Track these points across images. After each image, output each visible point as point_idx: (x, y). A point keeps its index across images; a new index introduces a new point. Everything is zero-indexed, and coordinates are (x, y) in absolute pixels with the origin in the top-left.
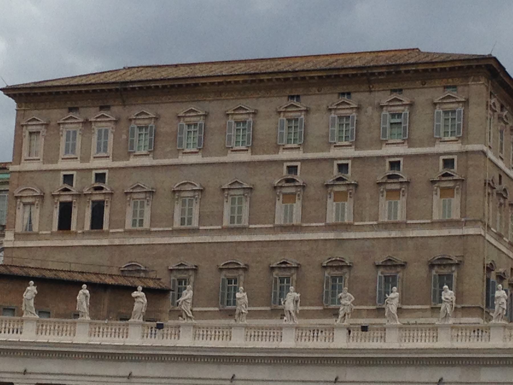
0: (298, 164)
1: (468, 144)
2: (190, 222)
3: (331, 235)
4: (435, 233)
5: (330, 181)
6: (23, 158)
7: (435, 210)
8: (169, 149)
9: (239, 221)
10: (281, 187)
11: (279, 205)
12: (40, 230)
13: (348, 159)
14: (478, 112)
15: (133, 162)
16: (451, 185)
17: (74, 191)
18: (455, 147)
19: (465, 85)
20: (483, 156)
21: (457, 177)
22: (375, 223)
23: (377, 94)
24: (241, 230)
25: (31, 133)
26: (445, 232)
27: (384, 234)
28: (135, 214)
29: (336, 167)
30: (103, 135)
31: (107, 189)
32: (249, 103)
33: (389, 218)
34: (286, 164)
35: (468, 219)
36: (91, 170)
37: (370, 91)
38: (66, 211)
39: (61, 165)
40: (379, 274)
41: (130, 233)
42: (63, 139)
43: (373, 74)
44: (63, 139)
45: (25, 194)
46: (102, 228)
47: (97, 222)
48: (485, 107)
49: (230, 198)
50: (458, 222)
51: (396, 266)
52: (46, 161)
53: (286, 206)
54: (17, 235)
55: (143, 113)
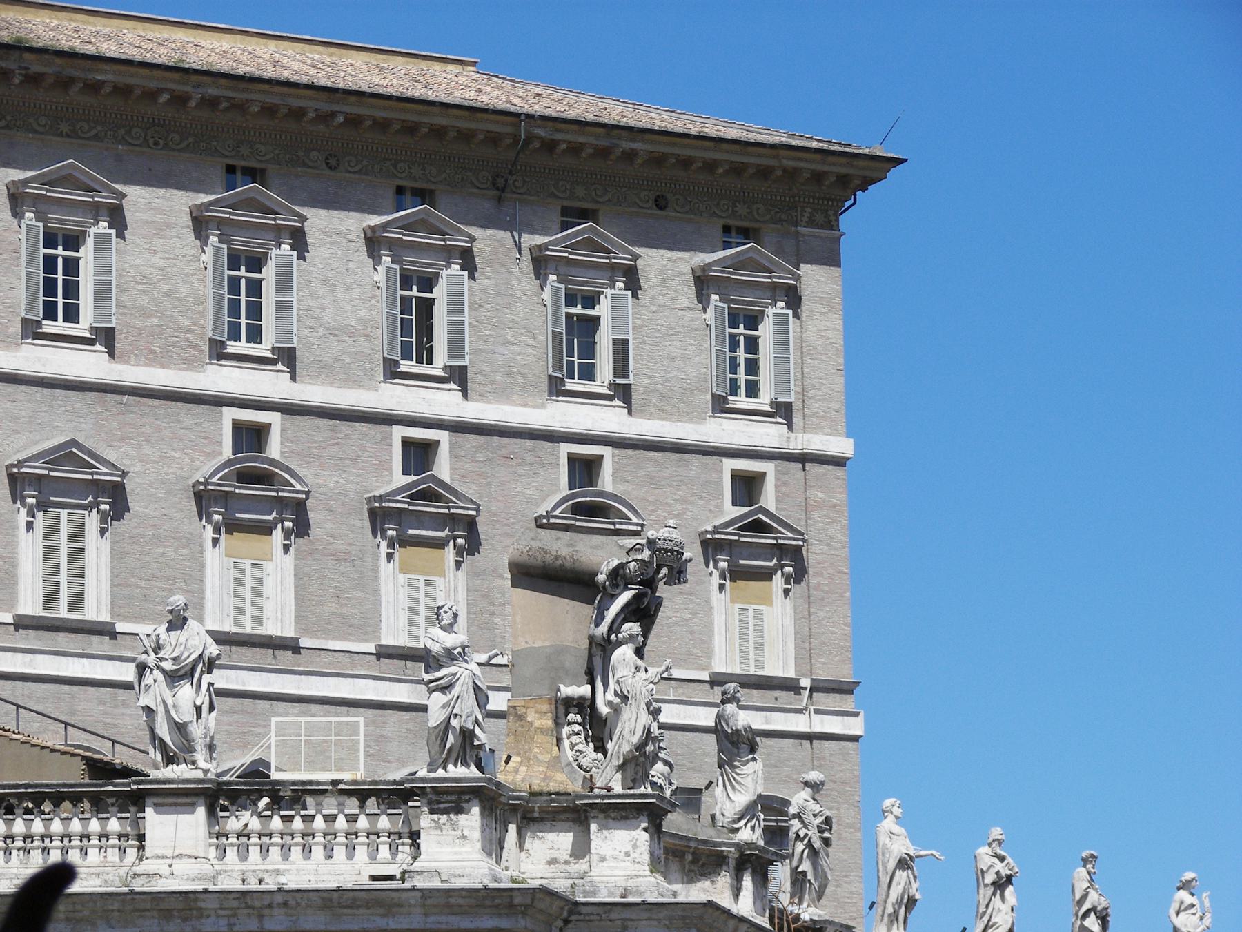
1: (805, 429)
7: (718, 643)
18: (769, 435)
50: (790, 686)
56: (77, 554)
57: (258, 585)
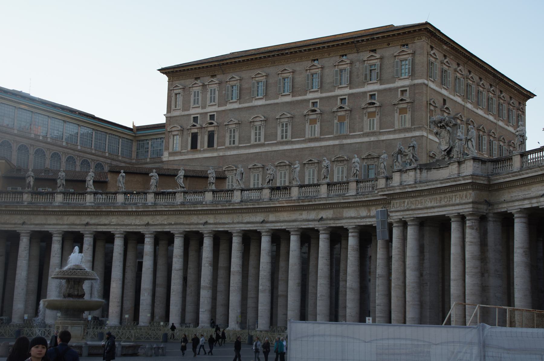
0: (318, 101)
2: (259, 140)
3: (337, 142)
4: (397, 136)
5: (335, 109)
6: (172, 109)
7: (396, 123)
8: (247, 98)
9: (286, 138)
10: (308, 115)
11: (307, 125)
12: (181, 150)
13: (346, 95)
14: (421, 60)
15: (229, 106)
16: (405, 106)
17: (198, 126)
18: (407, 82)
19: (413, 43)
20: (424, 86)
21: (408, 100)
22: (362, 133)
23: (361, 54)
24: (287, 143)
25: (176, 94)
26: (402, 135)
27: (366, 139)
28: (230, 136)
29: (339, 101)
30: (213, 92)
31: (215, 124)
32: (289, 67)
33: (370, 129)
34: (311, 101)
35: (415, 126)
36: (207, 113)
37: (358, 52)
38: (194, 137)
39: (192, 111)
40: (364, 164)
41: (229, 148)
42: (192, 96)
43: (358, 41)
44: (192, 96)
45: (173, 129)
46: (213, 146)
47: (211, 144)
48: (426, 55)
49: (281, 124)
51: (374, 158)
52: (184, 110)
53: (312, 127)
54: (171, 154)
55: (233, 77)
56: (286, 130)
57: (315, 129)
